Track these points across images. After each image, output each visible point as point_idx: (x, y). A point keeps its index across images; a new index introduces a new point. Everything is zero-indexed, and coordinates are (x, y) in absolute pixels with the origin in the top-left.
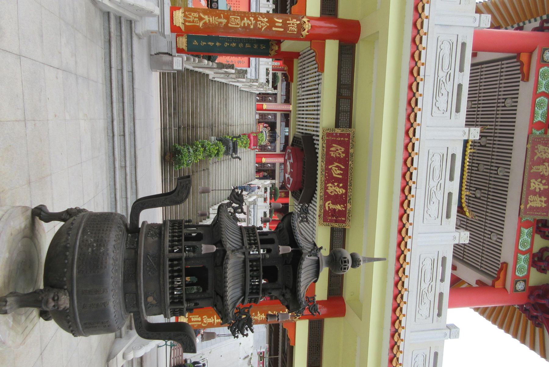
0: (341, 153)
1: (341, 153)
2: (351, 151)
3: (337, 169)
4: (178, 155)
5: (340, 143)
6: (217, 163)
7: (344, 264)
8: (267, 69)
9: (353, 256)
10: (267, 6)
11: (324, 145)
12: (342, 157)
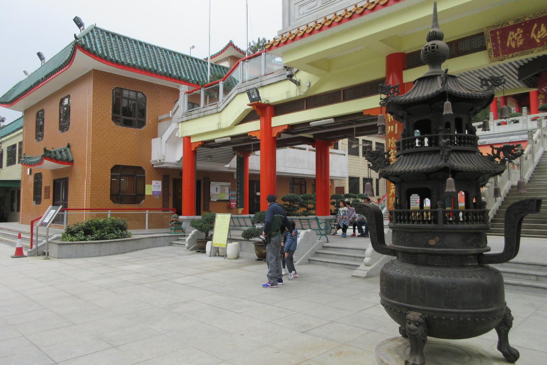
0: (516, 34)
1: (516, 34)
2: (511, 23)
3: (539, 32)
5: (504, 38)
7: (428, 51)
8: (499, 124)
9: (430, 39)
11: (510, 55)
12: (522, 31)
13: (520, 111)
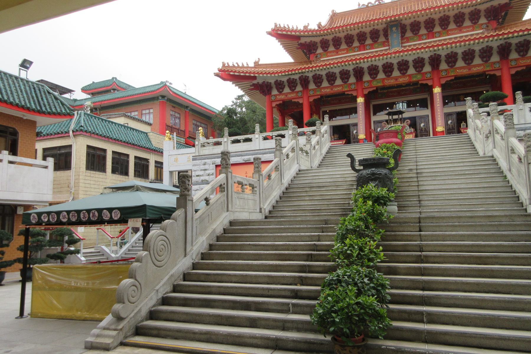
4: (334, 323)
6: (422, 198)
10: (226, 143)
13: (284, 125)
